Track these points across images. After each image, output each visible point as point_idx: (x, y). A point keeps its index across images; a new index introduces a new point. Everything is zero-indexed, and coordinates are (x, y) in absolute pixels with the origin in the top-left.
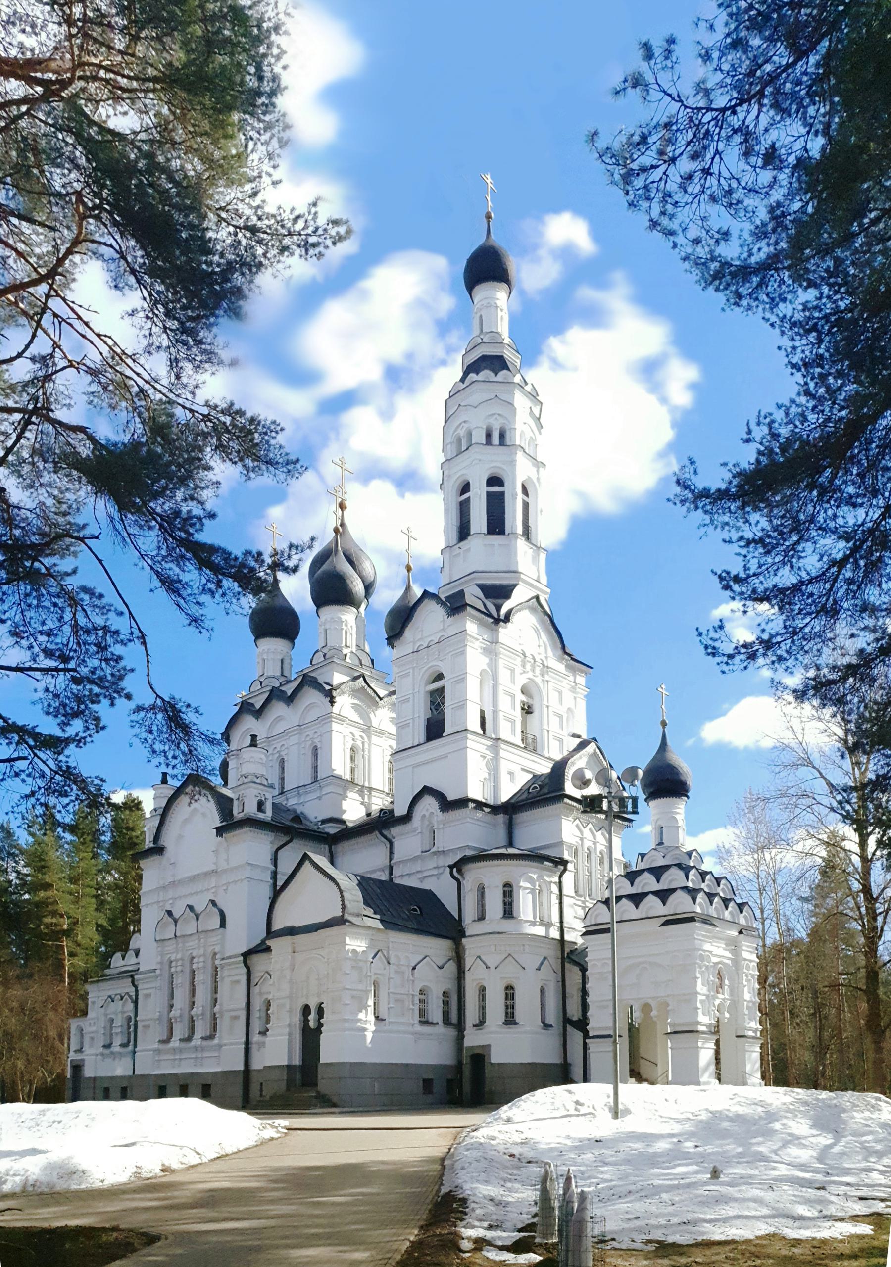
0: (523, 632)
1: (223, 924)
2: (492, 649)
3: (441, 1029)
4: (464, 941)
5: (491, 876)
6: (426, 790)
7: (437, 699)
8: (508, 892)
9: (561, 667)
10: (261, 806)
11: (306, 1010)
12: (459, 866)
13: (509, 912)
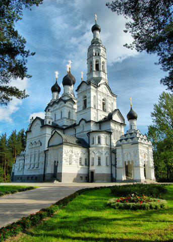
0: (103, 88)
1: (41, 145)
2: (97, 92)
3: (84, 166)
4: (90, 148)
5: (96, 136)
7: (85, 102)
9: (111, 95)
10: (49, 122)
11: (55, 162)
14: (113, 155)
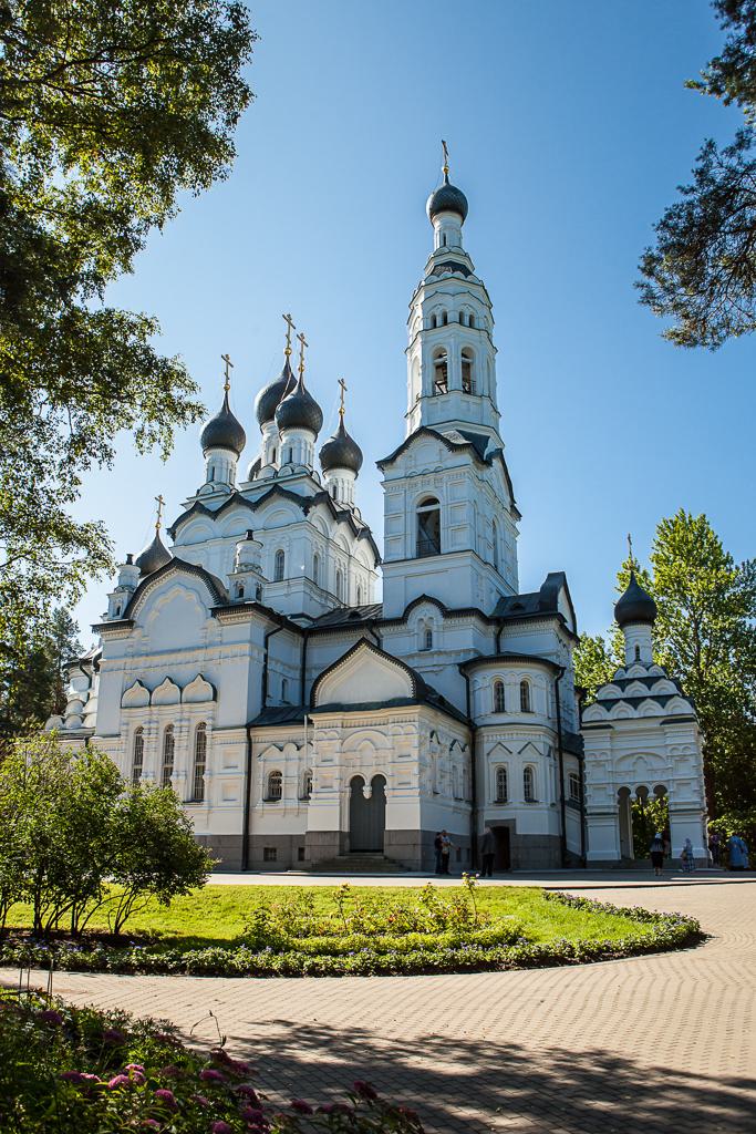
6: (424, 598)
8: (524, 687)
11: (357, 783)
12: (467, 668)
13: (525, 708)
14: (570, 763)
